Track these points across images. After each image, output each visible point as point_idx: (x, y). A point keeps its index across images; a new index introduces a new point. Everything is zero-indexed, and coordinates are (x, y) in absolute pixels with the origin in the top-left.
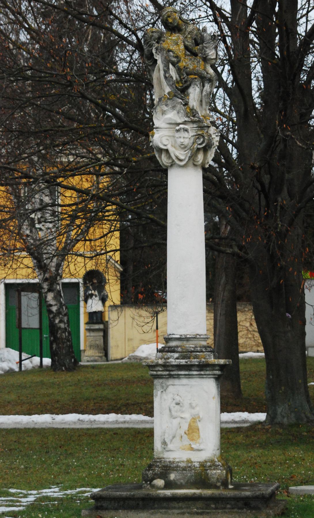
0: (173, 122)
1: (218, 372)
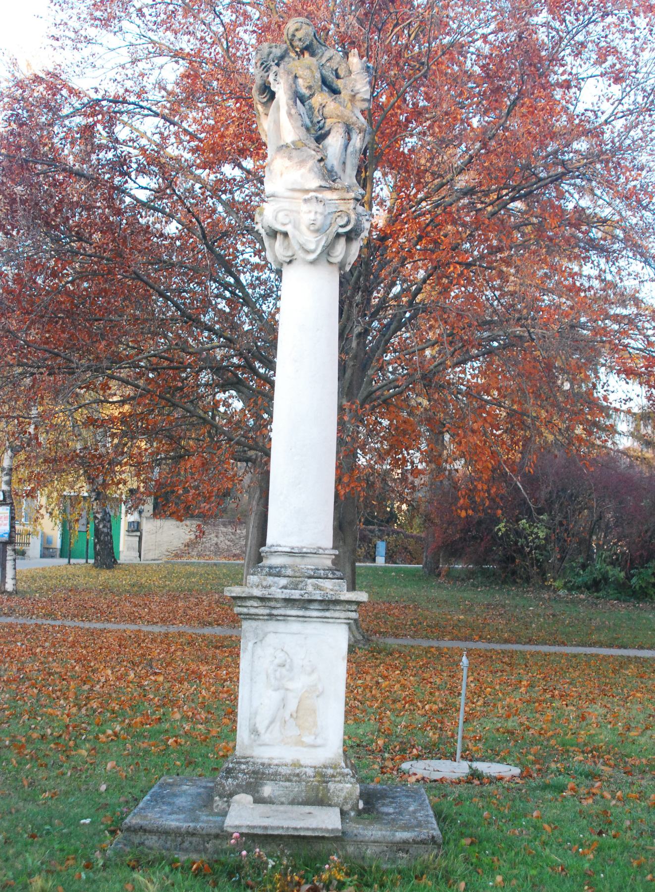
0: (299, 187)
1: (354, 615)
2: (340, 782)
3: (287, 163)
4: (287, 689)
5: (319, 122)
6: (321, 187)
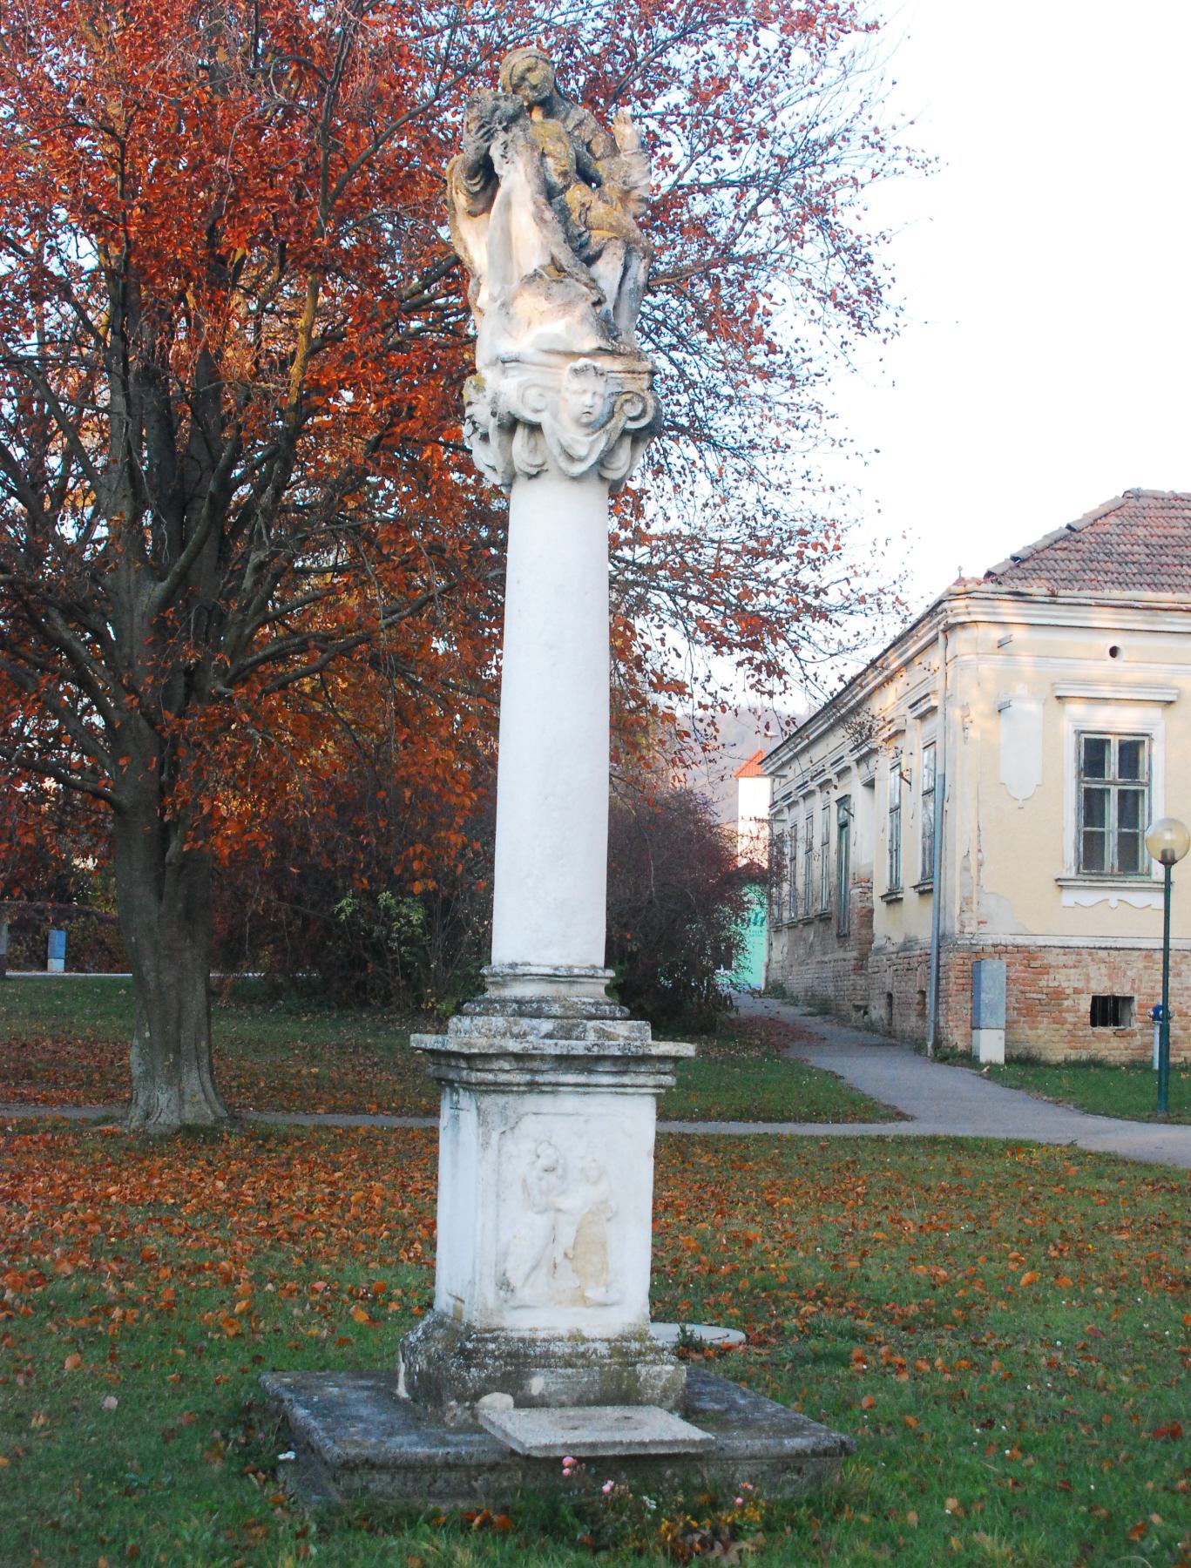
0: (561, 348)
1: (669, 1080)
2: (653, 1362)
3: (545, 305)
4: (559, 1210)
5: (580, 235)
6: (600, 349)
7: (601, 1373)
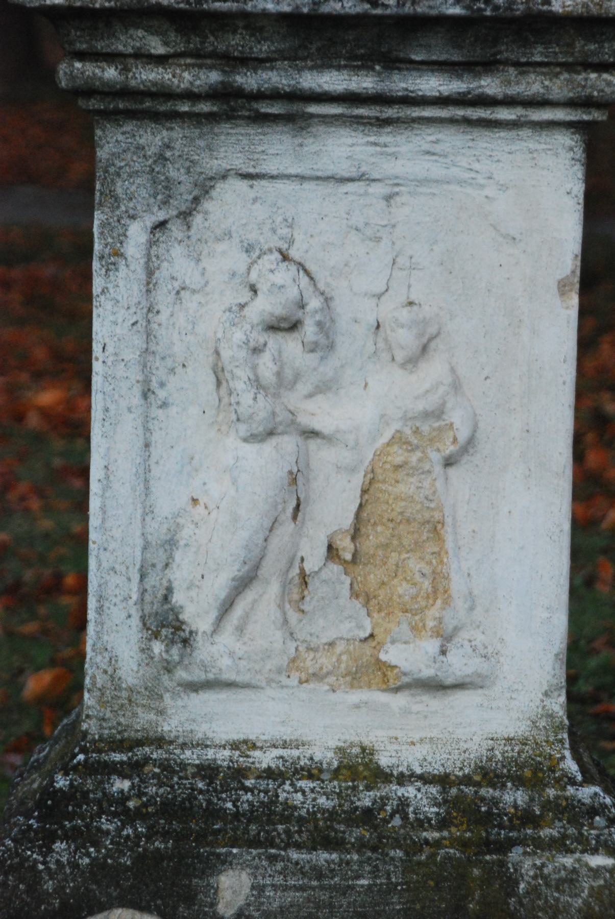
2: (560, 845)
4: (311, 434)
7: (408, 866)
